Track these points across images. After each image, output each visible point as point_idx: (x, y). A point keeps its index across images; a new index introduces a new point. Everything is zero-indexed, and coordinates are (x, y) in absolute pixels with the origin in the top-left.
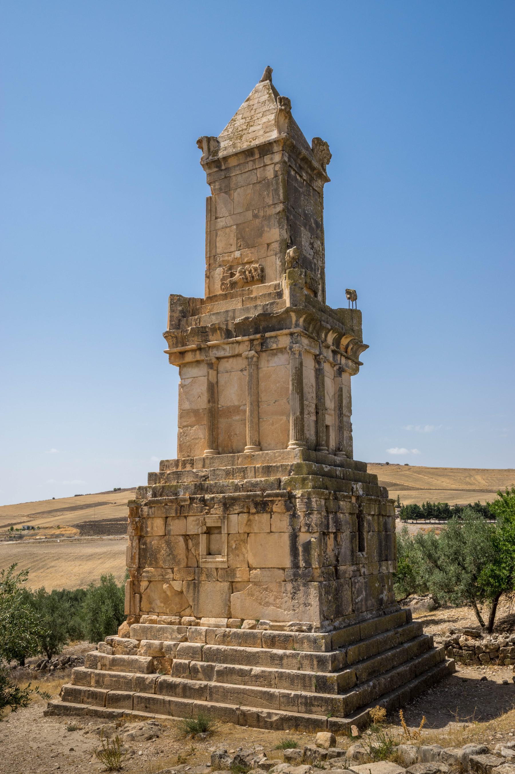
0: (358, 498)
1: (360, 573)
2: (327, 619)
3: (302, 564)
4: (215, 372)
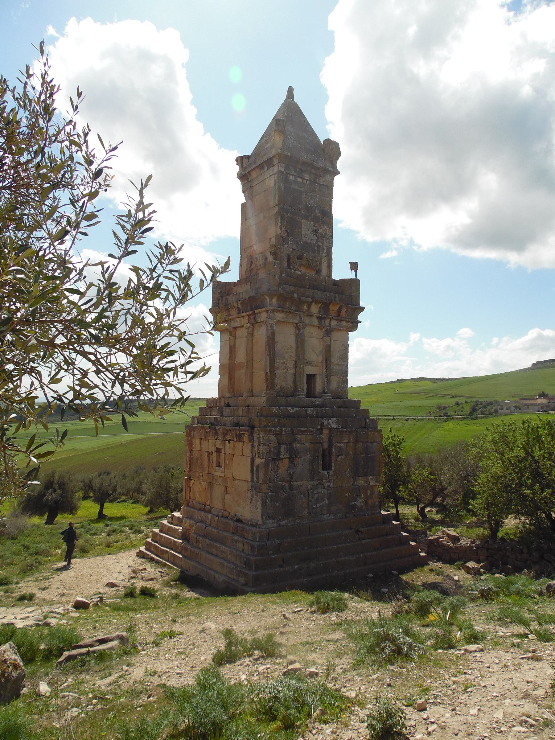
0: (330, 430)
1: (324, 486)
2: (273, 519)
3: (255, 480)
4: (233, 338)
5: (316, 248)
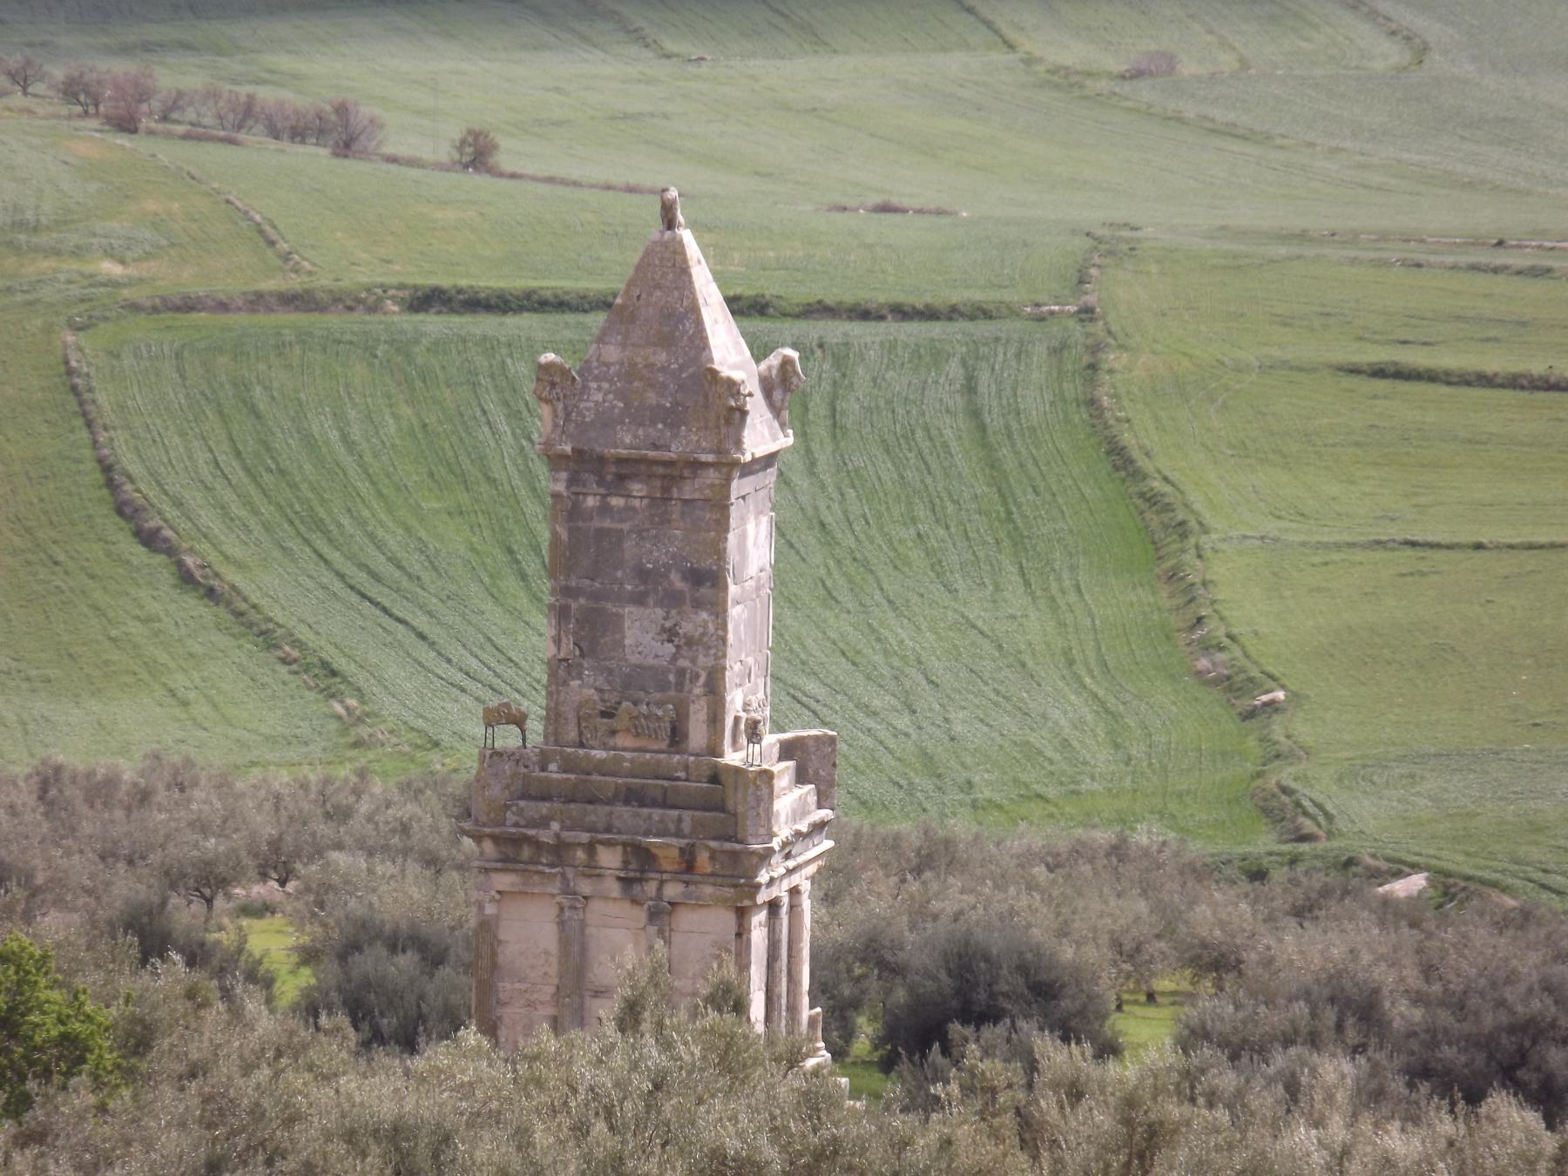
5: (672, 678)
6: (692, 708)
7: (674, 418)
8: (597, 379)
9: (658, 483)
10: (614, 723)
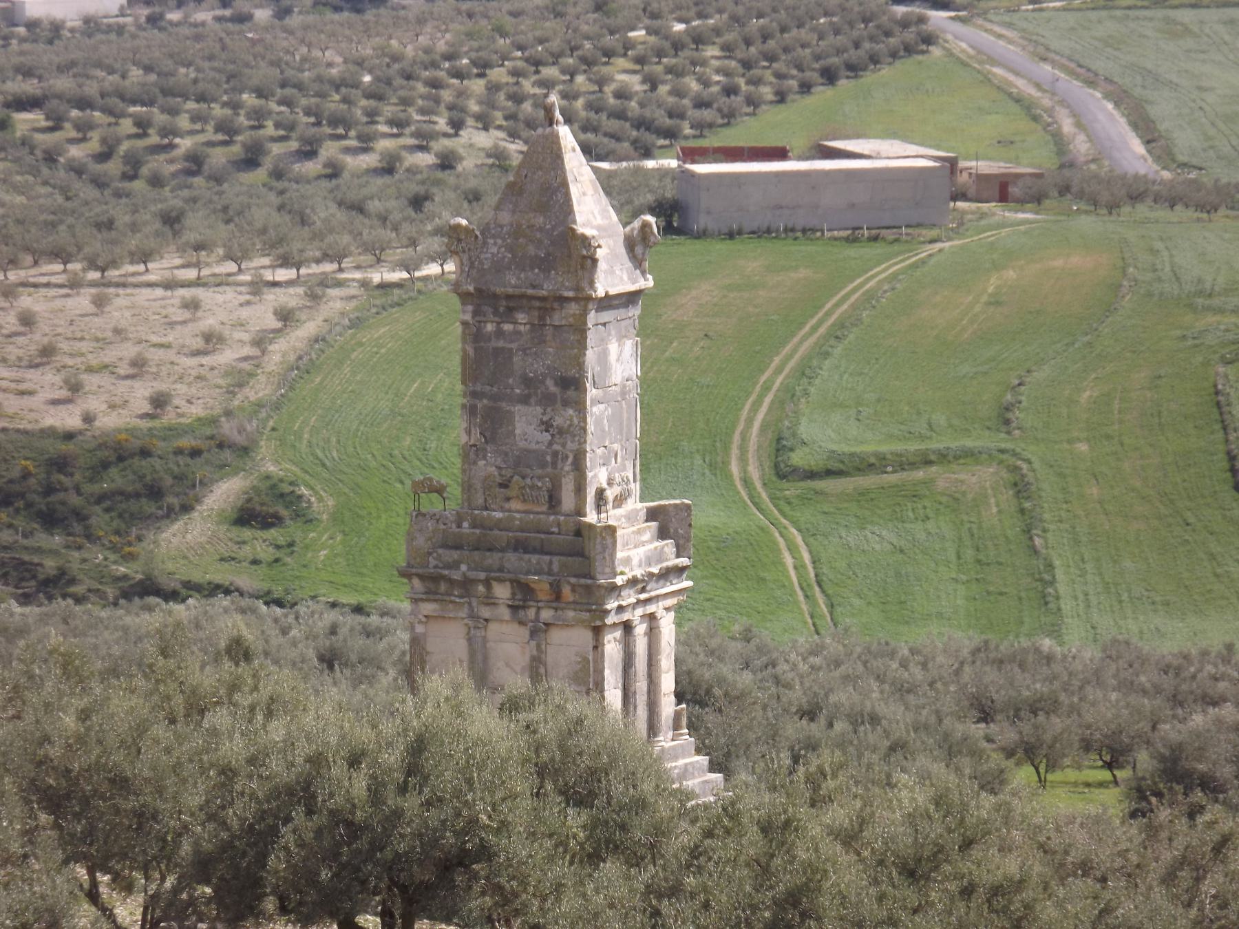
5: (549, 458)
6: (563, 480)
7: (546, 264)
8: (493, 237)
9: (536, 313)
10: (509, 493)
